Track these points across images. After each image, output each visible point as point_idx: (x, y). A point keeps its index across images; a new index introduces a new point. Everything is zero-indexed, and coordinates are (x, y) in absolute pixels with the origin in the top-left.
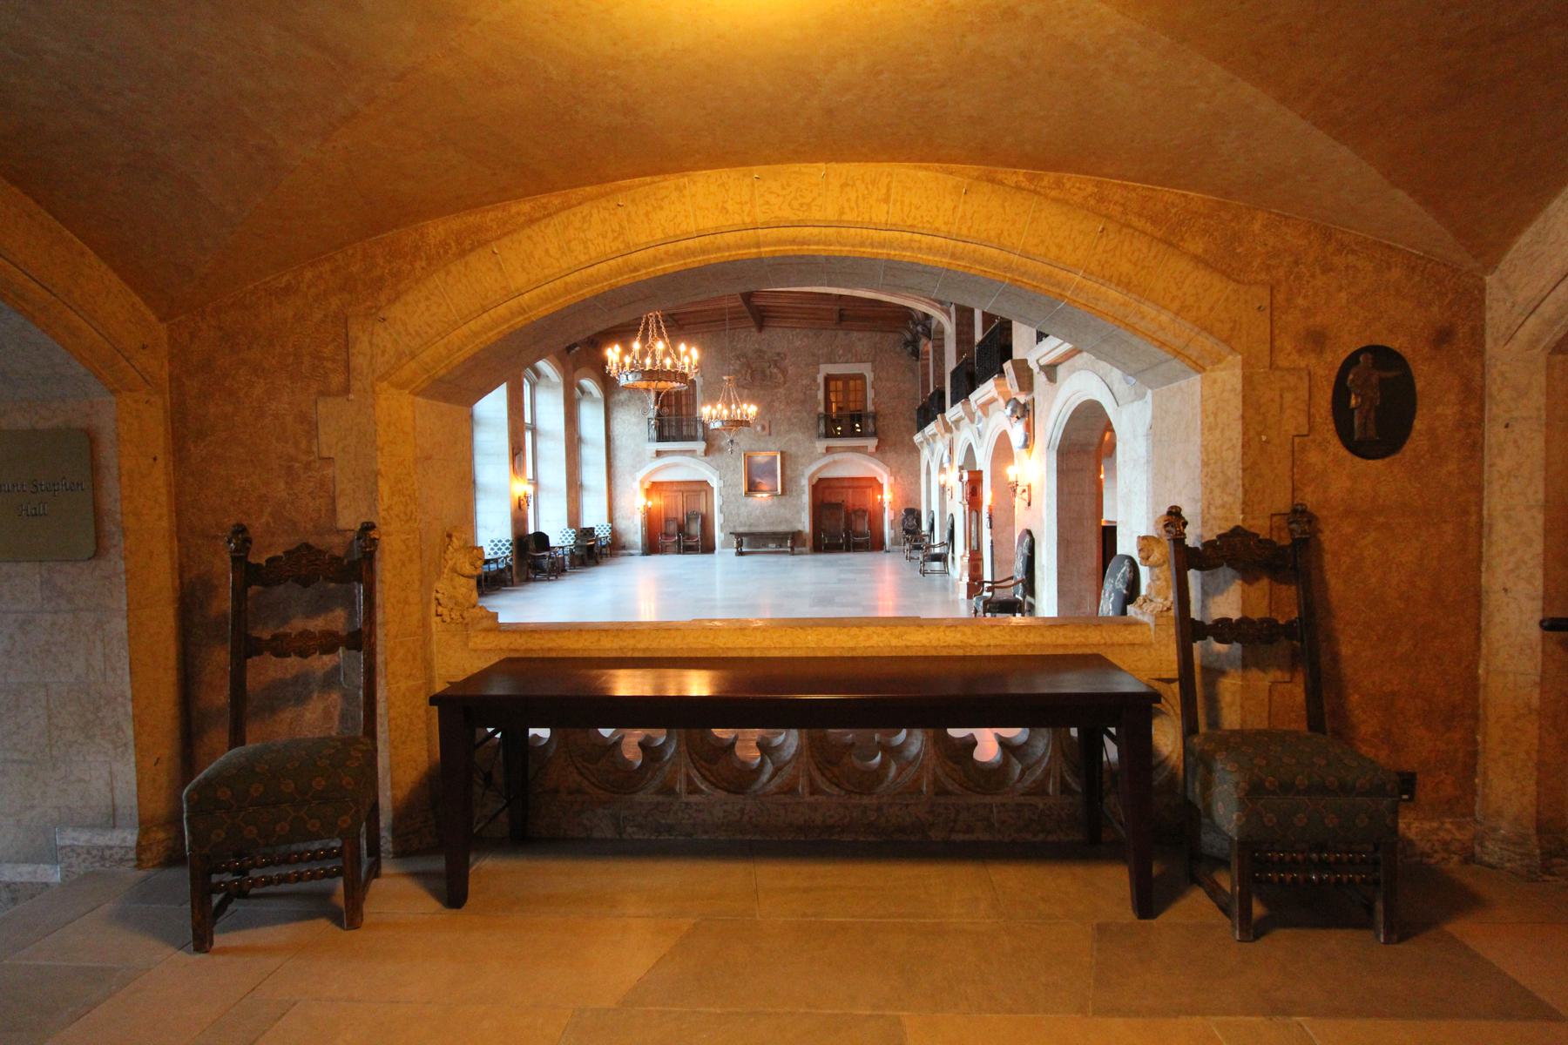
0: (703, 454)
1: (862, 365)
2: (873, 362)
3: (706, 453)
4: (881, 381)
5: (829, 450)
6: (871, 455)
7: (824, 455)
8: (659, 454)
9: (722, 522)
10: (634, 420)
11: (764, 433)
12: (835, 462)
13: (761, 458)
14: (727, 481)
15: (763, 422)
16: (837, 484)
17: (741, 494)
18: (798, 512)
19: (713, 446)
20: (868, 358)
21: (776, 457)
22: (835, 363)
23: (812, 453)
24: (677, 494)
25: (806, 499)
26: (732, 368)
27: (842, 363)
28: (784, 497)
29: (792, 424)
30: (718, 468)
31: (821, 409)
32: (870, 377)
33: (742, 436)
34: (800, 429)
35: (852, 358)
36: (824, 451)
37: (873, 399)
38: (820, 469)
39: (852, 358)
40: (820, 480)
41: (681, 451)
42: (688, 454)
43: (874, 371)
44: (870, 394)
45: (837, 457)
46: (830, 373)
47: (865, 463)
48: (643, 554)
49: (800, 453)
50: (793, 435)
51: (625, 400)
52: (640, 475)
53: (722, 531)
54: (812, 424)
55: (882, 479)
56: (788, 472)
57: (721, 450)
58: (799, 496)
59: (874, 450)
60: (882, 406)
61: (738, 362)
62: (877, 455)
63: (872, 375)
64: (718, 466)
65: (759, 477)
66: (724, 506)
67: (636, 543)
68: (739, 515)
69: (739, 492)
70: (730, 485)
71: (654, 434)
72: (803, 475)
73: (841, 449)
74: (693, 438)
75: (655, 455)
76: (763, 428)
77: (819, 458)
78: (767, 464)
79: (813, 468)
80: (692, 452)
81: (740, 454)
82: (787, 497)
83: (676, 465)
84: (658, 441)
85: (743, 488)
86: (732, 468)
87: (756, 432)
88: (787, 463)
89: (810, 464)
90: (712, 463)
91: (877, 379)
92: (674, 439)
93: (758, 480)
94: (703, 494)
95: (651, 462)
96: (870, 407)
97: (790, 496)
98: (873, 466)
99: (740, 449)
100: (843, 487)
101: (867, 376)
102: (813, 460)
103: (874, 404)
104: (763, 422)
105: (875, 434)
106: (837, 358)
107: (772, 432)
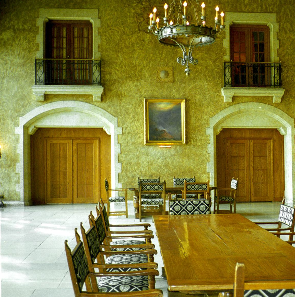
0: (99, 100)
1: (268, 15)
2: (278, 13)
3: (103, 98)
4: (286, 33)
5: (234, 98)
6: (276, 105)
7: (229, 105)
8: (47, 98)
9: (120, 171)
10: (18, 60)
11: (166, 80)
12: (240, 112)
13: (164, 106)
14: (126, 128)
15: (166, 68)
16: (236, 134)
17: (142, 143)
18: (203, 163)
19: (110, 90)
20: (273, 9)
21: (180, 104)
22: (242, 12)
23: (218, 101)
24: (66, 142)
25: (211, 149)
26: (133, 11)
27: (249, 12)
28: (188, 147)
29: (197, 72)
30: (115, 114)
31: (227, 58)
32: (273, 28)
33: (143, 82)
34: (205, 76)
35: (257, 7)
36: (230, 100)
37: (278, 49)
38: (225, 119)
39: (257, 7)
40: (224, 130)
41: (73, 96)
42: (80, 99)
43: (279, 22)
44: (274, 44)
45: (242, 107)
46: (236, 22)
47: (270, 113)
48: (25, 205)
49: (205, 102)
50: (198, 83)
51: (9, 39)
52: (23, 120)
53: (119, 181)
54: (218, 73)
55: (286, 131)
56: (193, 121)
57: (119, 96)
58: (204, 147)
59: (279, 101)
60: (287, 57)
61: (140, 5)
62: (281, 106)
63: (277, 26)
64: (116, 113)
65: (160, 124)
66: (123, 155)
67: (17, 194)
68: (138, 164)
69: (140, 140)
70: (129, 133)
71: (41, 75)
72: (208, 124)
73: (246, 99)
74: (87, 82)
75: (42, 99)
76: (167, 74)
77: (225, 108)
78: (170, 112)
79: (219, 117)
80: (87, 98)
81: (141, 101)
82: (192, 147)
83: (66, 111)
84: (46, 84)
85: (143, 137)
86: (131, 115)
87: (159, 78)
88: (192, 112)
89: (215, 113)
90: (109, 110)
91: (281, 30)
92: (65, 83)
93: (161, 128)
94: (96, 143)
95: (37, 106)
96: (274, 57)
97: (194, 146)
98: (277, 117)
99: (141, 96)
100: (245, 138)
101: (272, 26)
102: (218, 108)
103: (279, 55)
104: (166, 68)
105: (280, 85)
106: (243, 8)
107: (176, 79)
